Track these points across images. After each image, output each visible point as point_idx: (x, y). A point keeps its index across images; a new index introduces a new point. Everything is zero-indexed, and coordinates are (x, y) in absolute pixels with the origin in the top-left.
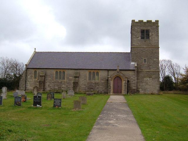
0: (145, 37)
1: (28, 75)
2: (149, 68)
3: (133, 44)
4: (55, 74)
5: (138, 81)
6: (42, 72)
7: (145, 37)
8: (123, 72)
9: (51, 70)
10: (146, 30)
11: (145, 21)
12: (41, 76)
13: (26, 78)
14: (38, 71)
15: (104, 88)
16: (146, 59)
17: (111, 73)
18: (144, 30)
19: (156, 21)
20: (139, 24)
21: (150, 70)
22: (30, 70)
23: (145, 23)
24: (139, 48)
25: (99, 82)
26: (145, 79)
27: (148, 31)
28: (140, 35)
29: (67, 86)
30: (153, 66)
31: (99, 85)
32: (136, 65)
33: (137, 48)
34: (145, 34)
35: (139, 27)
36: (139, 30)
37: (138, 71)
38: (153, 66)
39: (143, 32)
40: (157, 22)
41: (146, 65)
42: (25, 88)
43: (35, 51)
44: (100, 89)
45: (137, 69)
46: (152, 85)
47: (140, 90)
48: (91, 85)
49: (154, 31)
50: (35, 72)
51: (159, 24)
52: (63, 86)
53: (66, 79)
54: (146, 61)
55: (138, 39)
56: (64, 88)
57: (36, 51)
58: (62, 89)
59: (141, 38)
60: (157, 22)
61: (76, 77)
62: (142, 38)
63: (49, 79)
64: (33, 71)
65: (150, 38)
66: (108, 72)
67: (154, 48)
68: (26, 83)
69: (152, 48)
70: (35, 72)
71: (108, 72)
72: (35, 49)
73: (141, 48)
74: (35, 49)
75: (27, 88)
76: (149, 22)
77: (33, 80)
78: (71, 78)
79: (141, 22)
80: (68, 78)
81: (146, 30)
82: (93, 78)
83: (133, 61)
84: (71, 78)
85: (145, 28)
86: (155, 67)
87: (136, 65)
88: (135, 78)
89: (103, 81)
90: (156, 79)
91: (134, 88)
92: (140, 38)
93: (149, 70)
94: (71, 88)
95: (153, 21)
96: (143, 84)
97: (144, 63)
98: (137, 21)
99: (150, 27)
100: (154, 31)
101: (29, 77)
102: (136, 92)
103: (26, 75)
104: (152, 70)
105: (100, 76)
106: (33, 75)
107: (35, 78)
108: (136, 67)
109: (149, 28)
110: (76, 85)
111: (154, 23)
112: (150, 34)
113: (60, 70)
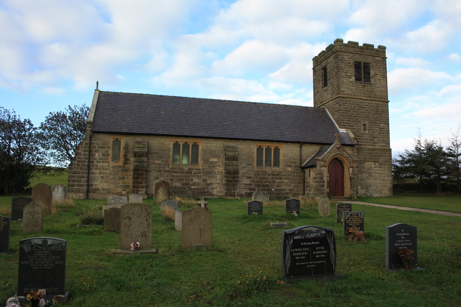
0: (363, 78)
1: (96, 151)
2: (374, 143)
4: (172, 149)
6: (139, 143)
7: (363, 78)
10: (364, 63)
13: (89, 158)
14: (123, 140)
15: (292, 185)
16: (367, 123)
18: (360, 63)
19: (379, 47)
20: (351, 50)
21: (375, 146)
22: (102, 136)
24: (353, 100)
25: (281, 170)
27: (367, 66)
28: (354, 73)
30: (379, 138)
31: (281, 179)
33: (348, 99)
34: (362, 71)
35: (351, 55)
36: (352, 62)
38: (379, 138)
39: (357, 66)
41: (366, 137)
42: (88, 185)
43: (97, 90)
44: (284, 187)
48: (264, 178)
49: (378, 67)
50: (117, 142)
52: (195, 180)
54: (367, 127)
55: (351, 80)
56: (198, 184)
57: (101, 88)
58: (193, 187)
62: (358, 79)
63: (156, 162)
64: (110, 139)
65: (372, 80)
66: (301, 147)
67: (380, 103)
68: (89, 173)
69: (377, 102)
70: (117, 142)
71: (301, 145)
73: (358, 101)
75: (93, 185)
77: (112, 164)
80: (206, 161)
81: (364, 63)
85: (362, 59)
86: (383, 140)
89: (289, 169)
90: (386, 167)
92: (353, 78)
93: (373, 147)
94: (214, 186)
96: (364, 175)
97: (362, 131)
99: (371, 58)
100: (378, 67)
101: (97, 155)
103: (90, 151)
104: (378, 146)
105: (284, 156)
106: (110, 152)
109: (369, 60)
111: (377, 50)
112: (372, 72)
113: (185, 140)
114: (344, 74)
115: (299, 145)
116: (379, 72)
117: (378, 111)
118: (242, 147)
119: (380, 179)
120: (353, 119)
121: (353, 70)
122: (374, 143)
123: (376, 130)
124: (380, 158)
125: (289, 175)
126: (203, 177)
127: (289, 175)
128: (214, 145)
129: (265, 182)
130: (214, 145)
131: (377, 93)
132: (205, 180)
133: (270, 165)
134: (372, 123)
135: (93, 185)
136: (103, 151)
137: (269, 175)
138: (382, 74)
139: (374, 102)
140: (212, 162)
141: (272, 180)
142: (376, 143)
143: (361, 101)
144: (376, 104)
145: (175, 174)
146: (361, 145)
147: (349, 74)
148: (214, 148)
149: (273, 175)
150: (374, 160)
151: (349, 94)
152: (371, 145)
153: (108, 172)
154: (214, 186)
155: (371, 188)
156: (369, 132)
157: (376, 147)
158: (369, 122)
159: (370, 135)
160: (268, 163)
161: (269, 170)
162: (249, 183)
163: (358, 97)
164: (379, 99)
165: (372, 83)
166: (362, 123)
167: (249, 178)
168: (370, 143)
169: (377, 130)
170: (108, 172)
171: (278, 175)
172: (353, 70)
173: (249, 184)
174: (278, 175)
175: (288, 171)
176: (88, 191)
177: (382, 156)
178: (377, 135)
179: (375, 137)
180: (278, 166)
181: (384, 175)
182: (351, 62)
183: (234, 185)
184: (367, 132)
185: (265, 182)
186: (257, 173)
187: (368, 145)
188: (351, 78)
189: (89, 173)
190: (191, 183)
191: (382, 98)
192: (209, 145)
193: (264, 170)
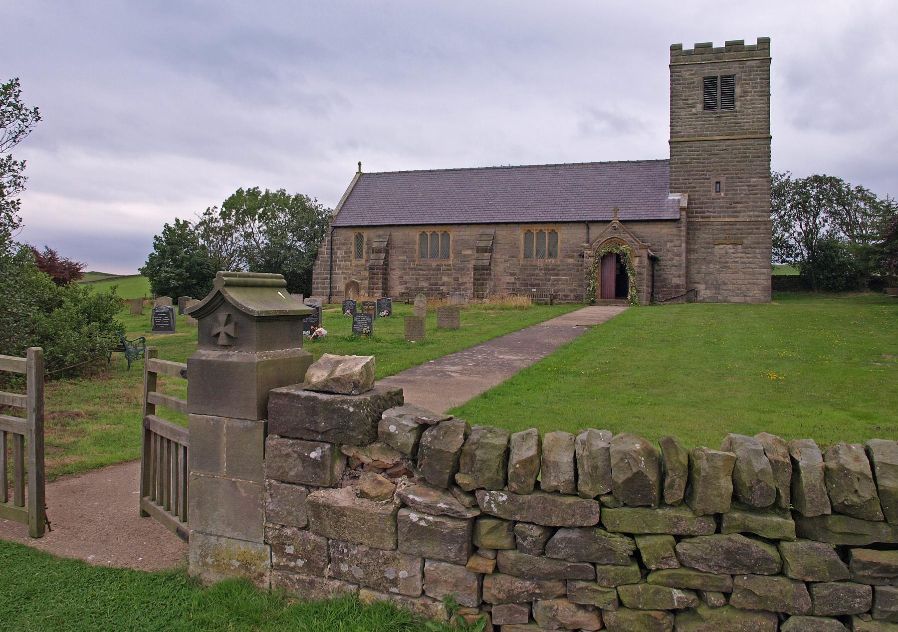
0: (719, 104)
1: (338, 249)
2: (736, 212)
3: (679, 129)
4: (418, 242)
5: (693, 256)
6: (379, 236)
7: (719, 104)
8: (638, 229)
9: (407, 231)
10: (722, 77)
11: (719, 44)
12: (377, 251)
13: (331, 257)
14: (366, 234)
16: (722, 179)
17: (595, 231)
18: (715, 78)
20: (697, 59)
21: (737, 217)
22: (344, 231)
23: (719, 50)
24: (698, 144)
25: (559, 263)
26: (718, 250)
27: (728, 81)
28: (701, 97)
29: (456, 279)
30: (747, 203)
31: (557, 275)
32: (684, 204)
33: (686, 144)
34: (719, 91)
35: (695, 68)
36: (698, 79)
37: (690, 221)
38: (747, 203)
39: (709, 84)
40: (765, 43)
41: (722, 202)
42: (331, 288)
44: (562, 287)
45: (688, 217)
46: (743, 271)
47: (701, 287)
48: (533, 275)
49: (750, 79)
50: (359, 238)
51: (773, 53)
52: (445, 279)
53: (452, 255)
54: (723, 186)
55: (694, 110)
56: (448, 284)
58: (441, 288)
59: (706, 108)
60: (765, 43)
61: (480, 250)
62: (709, 106)
63: (400, 258)
64: (352, 235)
65: (737, 104)
66: (588, 228)
67: (752, 141)
68: (331, 274)
69: (745, 142)
70: (359, 238)
71: (588, 228)
72: (360, 164)
73: (706, 144)
74: (360, 164)
75: (335, 287)
76: (735, 46)
77: (355, 262)
78: (469, 252)
79: (704, 48)
80: (458, 254)
81: (722, 77)
82: (538, 252)
83: (675, 189)
84: (469, 252)
85: (717, 72)
86: (754, 206)
87: (684, 204)
88: (680, 246)
89: (571, 261)
90: (757, 251)
91: (676, 281)
92: (699, 107)
93: (733, 220)
94: (467, 286)
95: (751, 41)
96: (712, 266)
97: (713, 194)
98: (688, 46)
99: (737, 65)
100: (750, 79)
101: (340, 253)
102: (690, 295)
104: (743, 216)
105: (562, 242)
107: (359, 255)
108: (682, 209)
109: (733, 69)
110: (482, 273)
111: (751, 48)
112: (738, 90)
113: (433, 229)
114: (681, 103)
115: (583, 226)
116: (753, 87)
117: (747, 157)
118: (504, 233)
119: (744, 273)
120: (696, 175)
121: (721, 84)
122: (736, 212)
123: (741, 190)
124: (744, 238)
125: (570, 270)
126: (454, 275)
127: (570, 270)
128: (468, 233)
129: (535, 279)
130: (468, 233)
131: (747, 126)
132: (456, 279)
133: (543, 256)
134: (732, 178)
135: (335, 287)
136: (345, 248)
137: (541, 270)
138: (759, 89)
139: (739, 143)
140: (465, 255)
141: (544, 278)
142: (739, 212)
143: (711, 143)
144: (742, 145)
145: (421, 272)
146: (709, 217)
147: (690, 102)
148: (467, 238)
149: (546, 270)
150: (733, 241)
151: (688, 136)
152: (729, 217)
153: (350, 272)
154: (467, 286)
155: (725, 288)
156: (726, 195)
157: (738, 220)
158: (727, 178)
159: (729, 198)
160: (434, 255)
161: (540, 262)
162: (513, 281)
163: (705, 138)
164: (750, 136)
165: (737, 108)
166: (713, 180)
167: (512, 275)
168: (726, 212)
169: (744, 190)
170: (350, 272)
171: (554, 270)
172: (721, 84)
173: (513, 283)
174: (554, 270)
175: (569, 264)
176: (331, 294)
177: (751, 234)
178: (742, 198)
179: (738, 203)
180: (556, 257)
181: (753, 266)
182: (695, 79)
183: (483, 285)
184: (722, 194)
185: (535, 279)
186: (523, 269)
187: (724, 217)
188: (694, 107)
189: (331, 274)
190: (440, 283)
191: (756, 133)
192: (461, 233)
193: (534, 263)
